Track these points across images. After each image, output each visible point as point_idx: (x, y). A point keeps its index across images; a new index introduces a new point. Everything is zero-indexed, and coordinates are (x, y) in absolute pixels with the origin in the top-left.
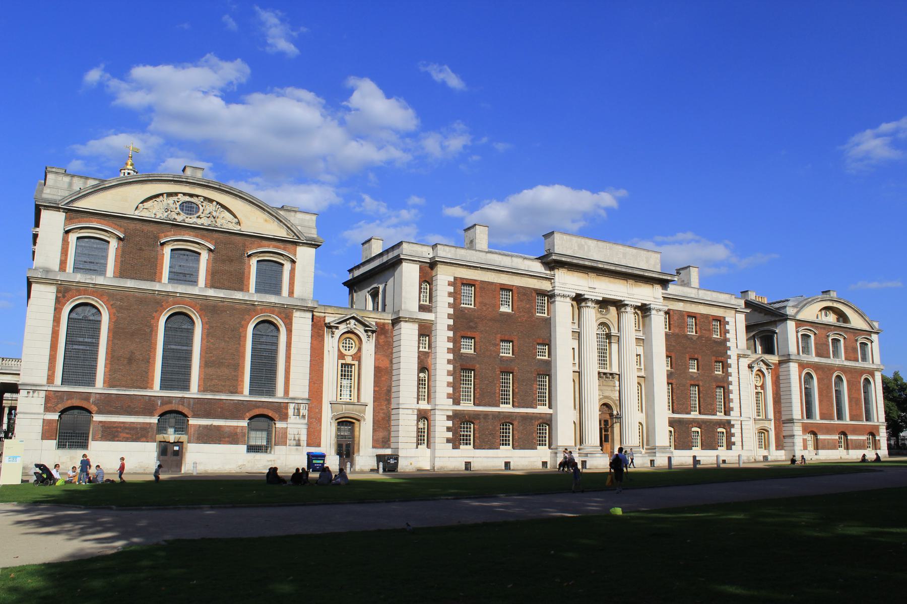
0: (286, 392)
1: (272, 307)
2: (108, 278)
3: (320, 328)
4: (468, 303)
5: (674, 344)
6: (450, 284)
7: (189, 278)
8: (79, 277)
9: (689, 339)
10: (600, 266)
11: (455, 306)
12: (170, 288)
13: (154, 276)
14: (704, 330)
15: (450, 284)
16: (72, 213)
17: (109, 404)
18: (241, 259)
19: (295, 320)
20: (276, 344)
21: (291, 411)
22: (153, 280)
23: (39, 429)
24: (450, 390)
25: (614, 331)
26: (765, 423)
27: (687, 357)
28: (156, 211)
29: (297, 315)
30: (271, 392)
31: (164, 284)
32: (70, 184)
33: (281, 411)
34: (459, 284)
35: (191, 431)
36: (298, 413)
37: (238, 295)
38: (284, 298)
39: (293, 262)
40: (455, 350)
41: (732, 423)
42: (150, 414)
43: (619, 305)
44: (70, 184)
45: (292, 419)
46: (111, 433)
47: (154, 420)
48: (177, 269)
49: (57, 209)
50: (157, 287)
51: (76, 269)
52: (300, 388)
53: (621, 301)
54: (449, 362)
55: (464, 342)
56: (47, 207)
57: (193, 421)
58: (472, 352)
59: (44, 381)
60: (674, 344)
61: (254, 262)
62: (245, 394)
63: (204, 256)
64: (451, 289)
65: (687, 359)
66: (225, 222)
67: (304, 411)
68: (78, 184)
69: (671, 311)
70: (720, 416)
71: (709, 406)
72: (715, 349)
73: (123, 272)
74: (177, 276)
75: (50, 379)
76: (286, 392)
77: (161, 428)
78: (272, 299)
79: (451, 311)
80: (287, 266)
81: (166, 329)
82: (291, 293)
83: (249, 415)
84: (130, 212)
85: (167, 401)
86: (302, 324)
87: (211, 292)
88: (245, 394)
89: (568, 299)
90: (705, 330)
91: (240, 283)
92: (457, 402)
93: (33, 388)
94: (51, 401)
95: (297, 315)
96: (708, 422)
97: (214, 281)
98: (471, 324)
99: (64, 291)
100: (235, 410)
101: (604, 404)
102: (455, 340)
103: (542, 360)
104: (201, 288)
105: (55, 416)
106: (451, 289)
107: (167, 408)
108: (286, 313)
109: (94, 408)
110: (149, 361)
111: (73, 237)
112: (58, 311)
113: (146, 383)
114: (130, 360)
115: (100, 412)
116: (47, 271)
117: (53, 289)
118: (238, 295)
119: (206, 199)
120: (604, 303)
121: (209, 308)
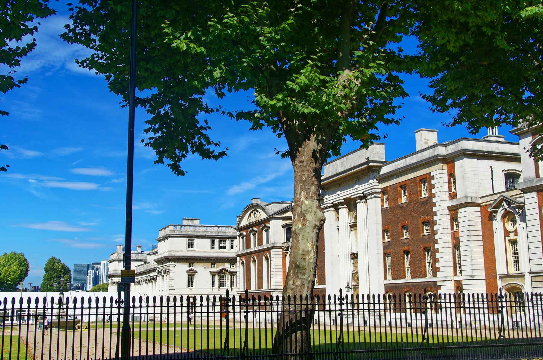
5: (390, 217)
9: (401, 208)
14: (412, 194)
19: (271, 253)
26: (515, 280)
27: (400, 225)
39: (270, 228)
41: (439, 284)
60: (390, 217)
65: (400, 227)
69: (389, 188)
70: (429, 278)
71: (418, 269)
72: (421, 210)
90: (413, 194)
96: (417, 285)
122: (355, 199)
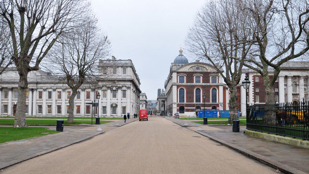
0: (219, 102)
1: (215, 86)
2: (185, 83)
3: (225, 89)
4: (257, 81)
6: (253, 77)
7: (199, 82)
8: (180, 84)
10: (292, 68)
11: (254, 81)
12: (196, 84)
13: (193, 82)
15: (253, 77)
16: (178, 73)
17: (187, 105)
18: (209, 77)
19: (220, 88)
20: (216, 93)
21: (220, 105)
22: (192, 83)
23: (176, 110)
24: (253, 100)
25: (297, 83)
28: (191, 70)
29: (220, 86)
30: (216, 102)
31: (195, 83)
32: (177, 67)
33: (218, 105)
34: (254, 77)
35: (201, 109)
36: (221, 105)
37: (208, 84)
38: (217, 84)
40: (254, 91)
42: (194, 107)
43: (299, 77)
44: (177, 67)
45: (220, 107)
46: (188, 110)
47: (195, 108)
48: (197, 80)
49: (175, 72)
50: (193, 84)
51: (180, 82)
52: (221, 101)
53: (299, 76)
54: (253, 94)
55: (256, 89)
56: (174, 72)
57: (201, 108)
58: (258, 91)
59: (176, 102)
61: (211, 77)
62: (211, 102)
63: (201, 77)
64: (253, 78)
66: (205, 71)
67: (222, 105)
68: (178, 67)
73: (187, 82)
74: (197, 82)
75: (177, 102)
76: (219, 102)
77: (196, 109)
78: (215, 84)
79: (253, 83)
80: (217, 77)
81: (196, 91)
82: (218, 82)
83: (212, 106)
84: (187, 71)
85: (197, 104)
86: (221, 88)
87: (203, 84)
88: (211, 102)
89: (283, 77)
91: (208, 82)
92: (255, 102)
93: (175, 103)
94: (178, 105)
95: (220, 86)
97: (204, 82)
98: (258, 85)
99: (178, 86)
100: (209, 105)
101: (295, 101)
102: (254, 89)
103: (277, 92)
104: (201, 83)
105: (179, 108)
106: (253, 78)
107: (197, 106)
108: (218, 86)
109: (184, 106)
110: (193, 97)
111: (178, 77)
112: (177, 90)
113: (193, 102)
114: (190, 98)
115: (186, 107)
116: (175, 83)
117: (176, 86)
118: (208, 84)
119: (200, 66)
120: (295, 77)
121: (203, 87)
122: (301, 77)
